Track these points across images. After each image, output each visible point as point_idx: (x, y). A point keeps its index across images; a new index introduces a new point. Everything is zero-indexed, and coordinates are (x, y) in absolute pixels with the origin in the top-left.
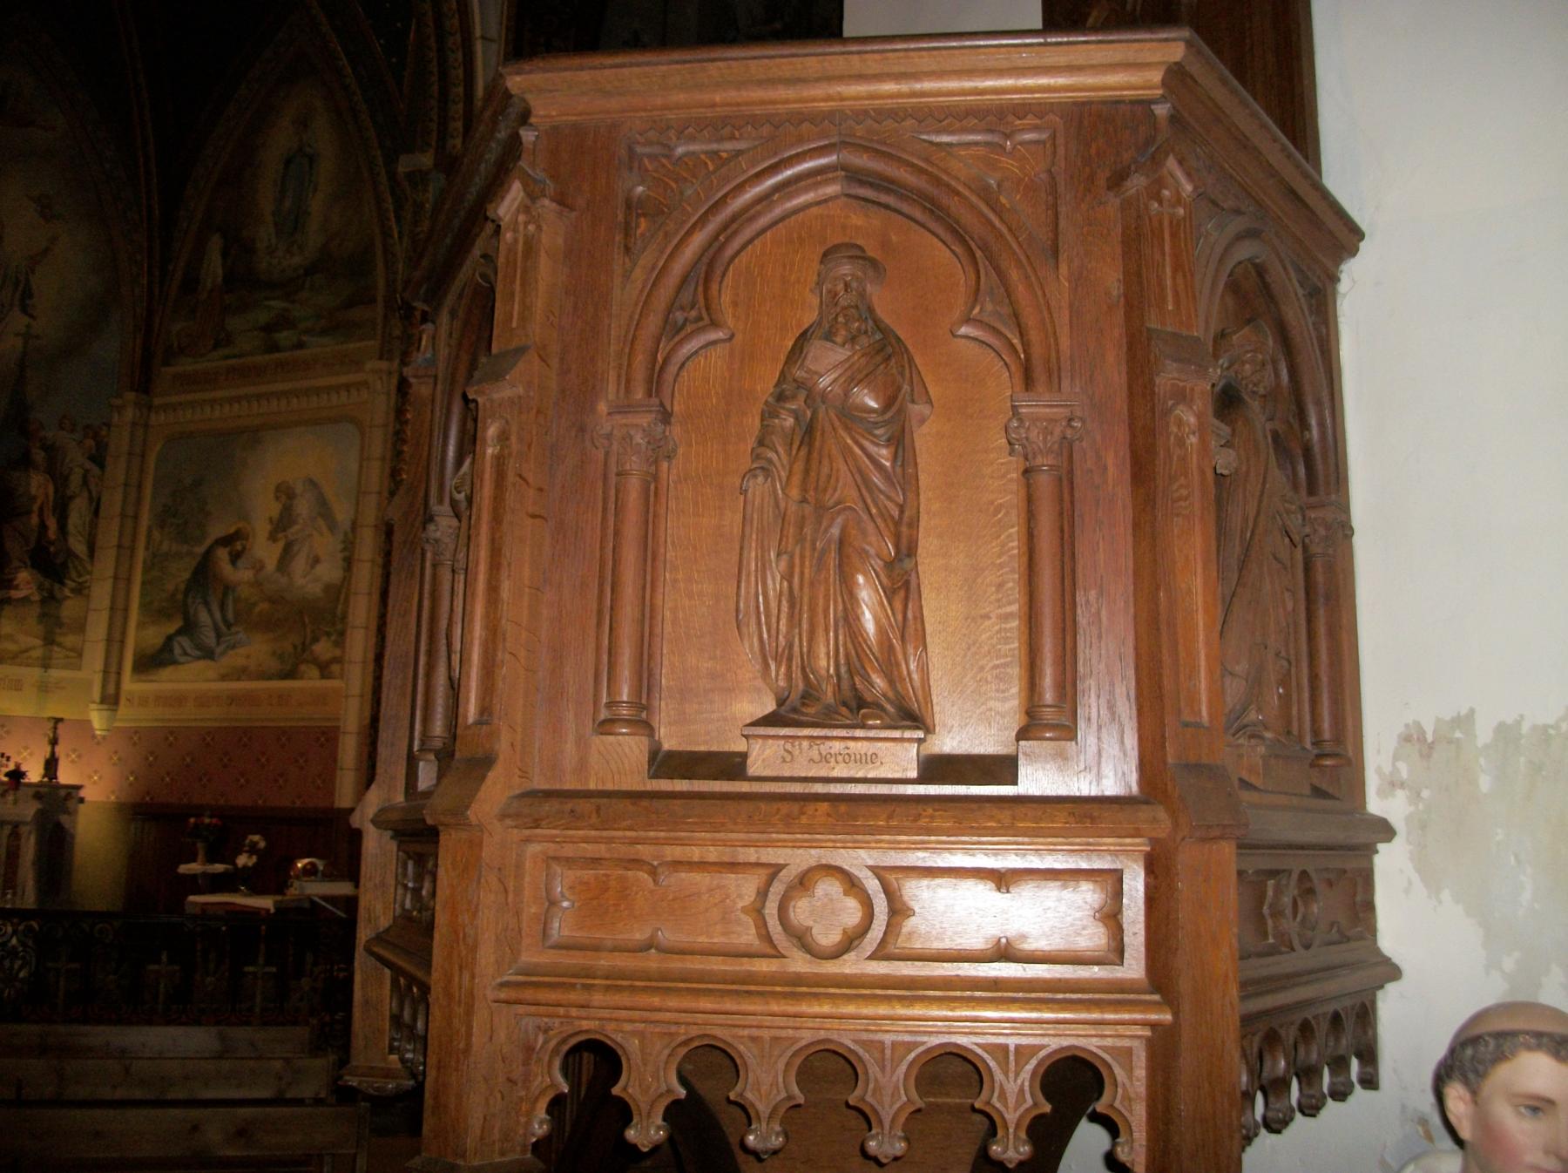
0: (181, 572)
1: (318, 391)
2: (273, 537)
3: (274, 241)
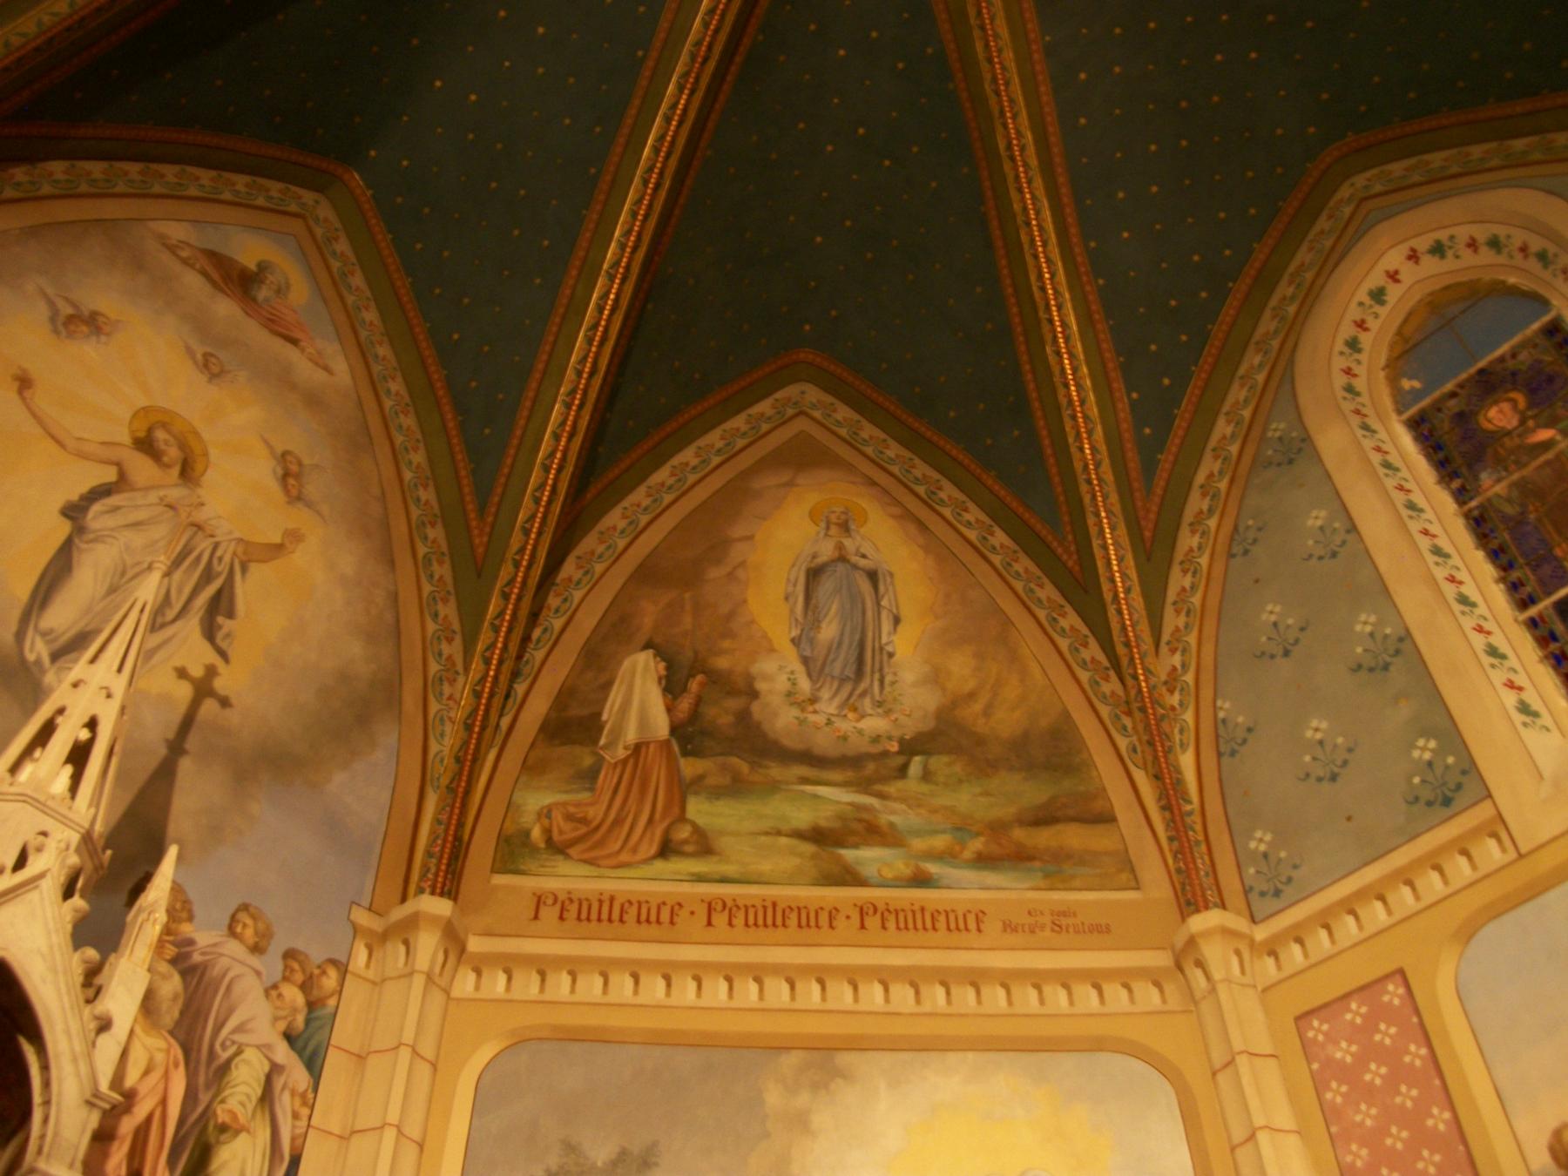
3: (805, 685)
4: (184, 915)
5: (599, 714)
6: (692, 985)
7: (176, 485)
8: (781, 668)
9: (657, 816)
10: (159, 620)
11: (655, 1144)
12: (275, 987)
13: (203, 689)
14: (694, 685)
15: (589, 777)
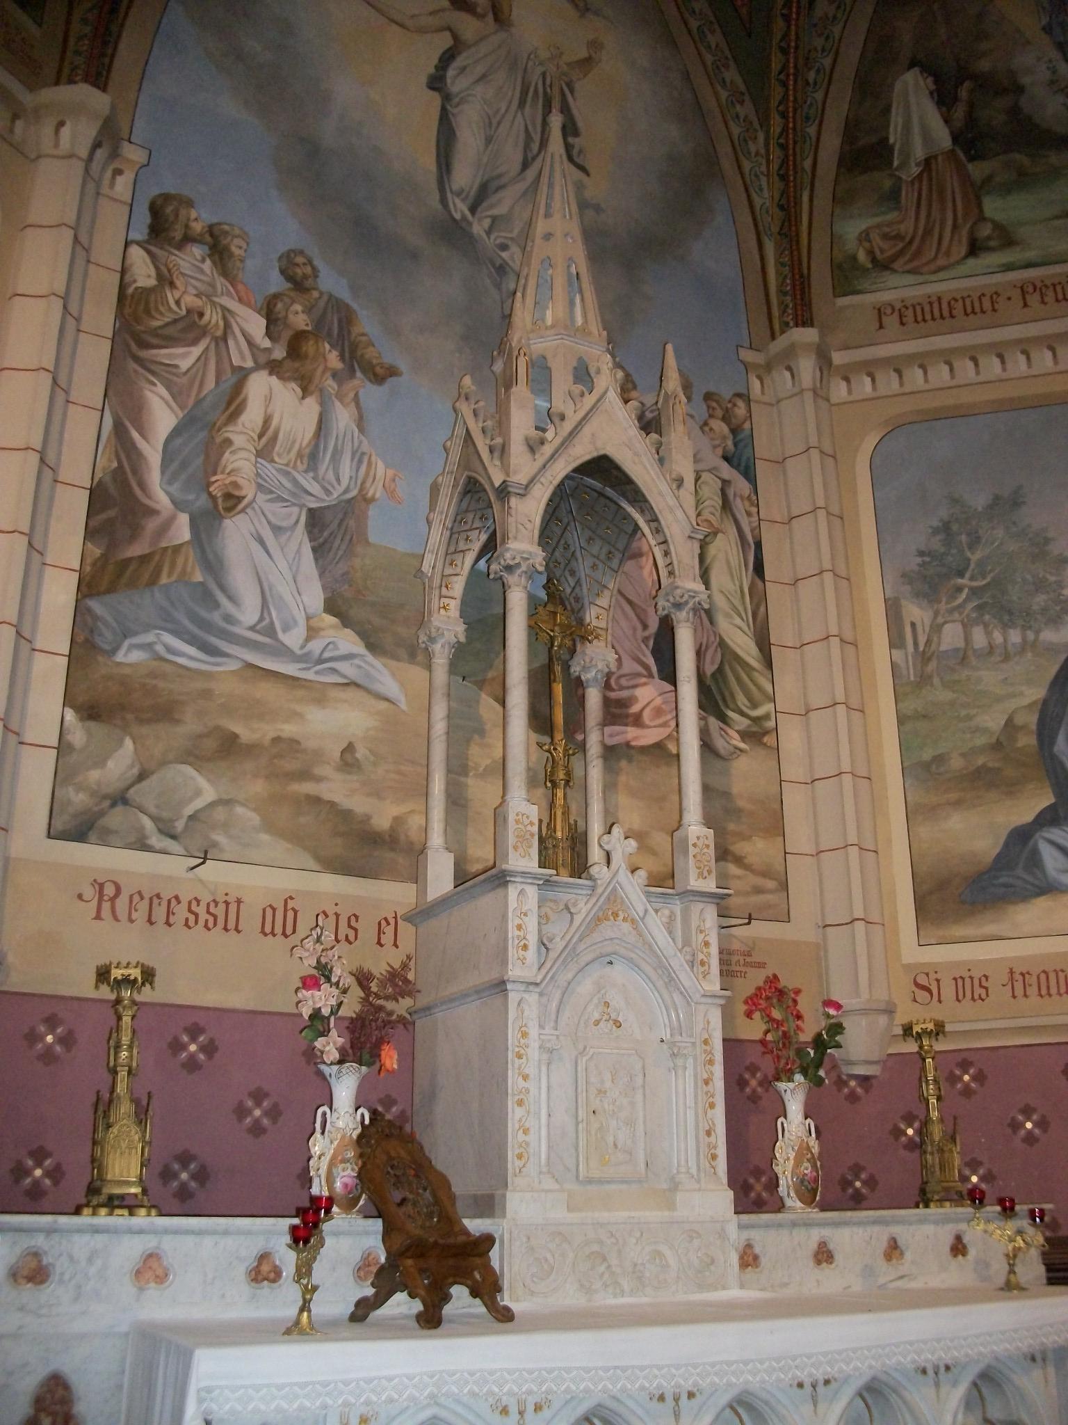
4: (630, 386)
5: (887, 139)
6: (1022, 358)
7: (495, 33)
8: (1039, 59)
9: (960, 221)
10: (530, 156)
11: (1020, 487)
12: (706, 424)
14: (963, 93)
15: (893, 197)
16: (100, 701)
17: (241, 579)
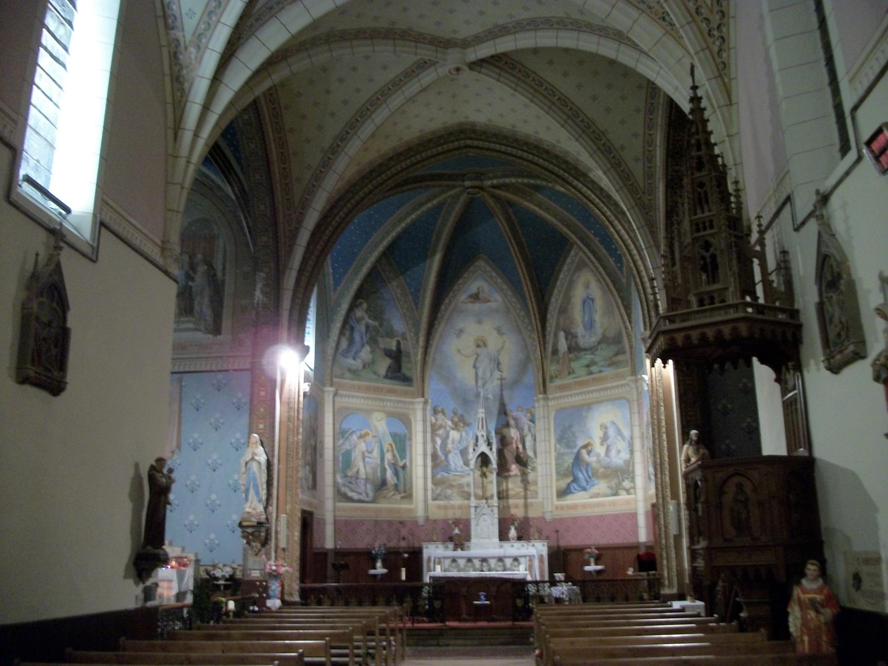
0: (569, 460)
1: (610, 388)
2: (602, 444)
13: (502, 379)
15: (558, 362)
16: (436, 483)
17: (451, 463)
